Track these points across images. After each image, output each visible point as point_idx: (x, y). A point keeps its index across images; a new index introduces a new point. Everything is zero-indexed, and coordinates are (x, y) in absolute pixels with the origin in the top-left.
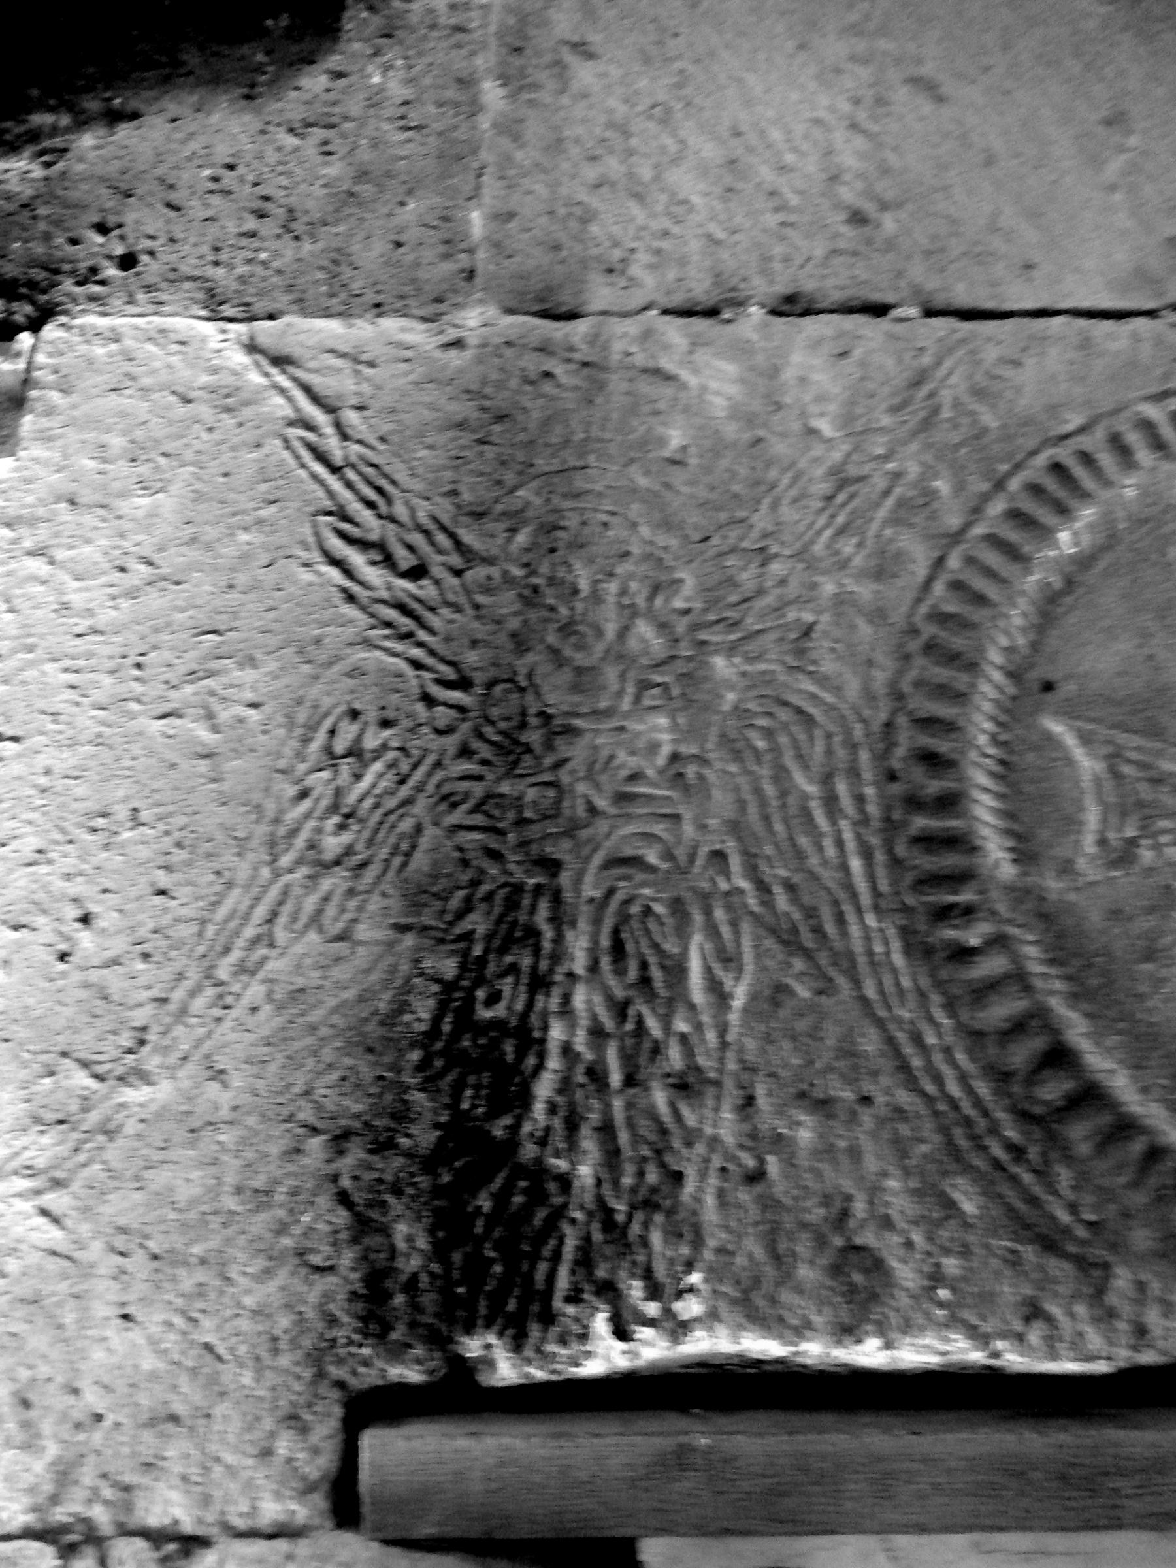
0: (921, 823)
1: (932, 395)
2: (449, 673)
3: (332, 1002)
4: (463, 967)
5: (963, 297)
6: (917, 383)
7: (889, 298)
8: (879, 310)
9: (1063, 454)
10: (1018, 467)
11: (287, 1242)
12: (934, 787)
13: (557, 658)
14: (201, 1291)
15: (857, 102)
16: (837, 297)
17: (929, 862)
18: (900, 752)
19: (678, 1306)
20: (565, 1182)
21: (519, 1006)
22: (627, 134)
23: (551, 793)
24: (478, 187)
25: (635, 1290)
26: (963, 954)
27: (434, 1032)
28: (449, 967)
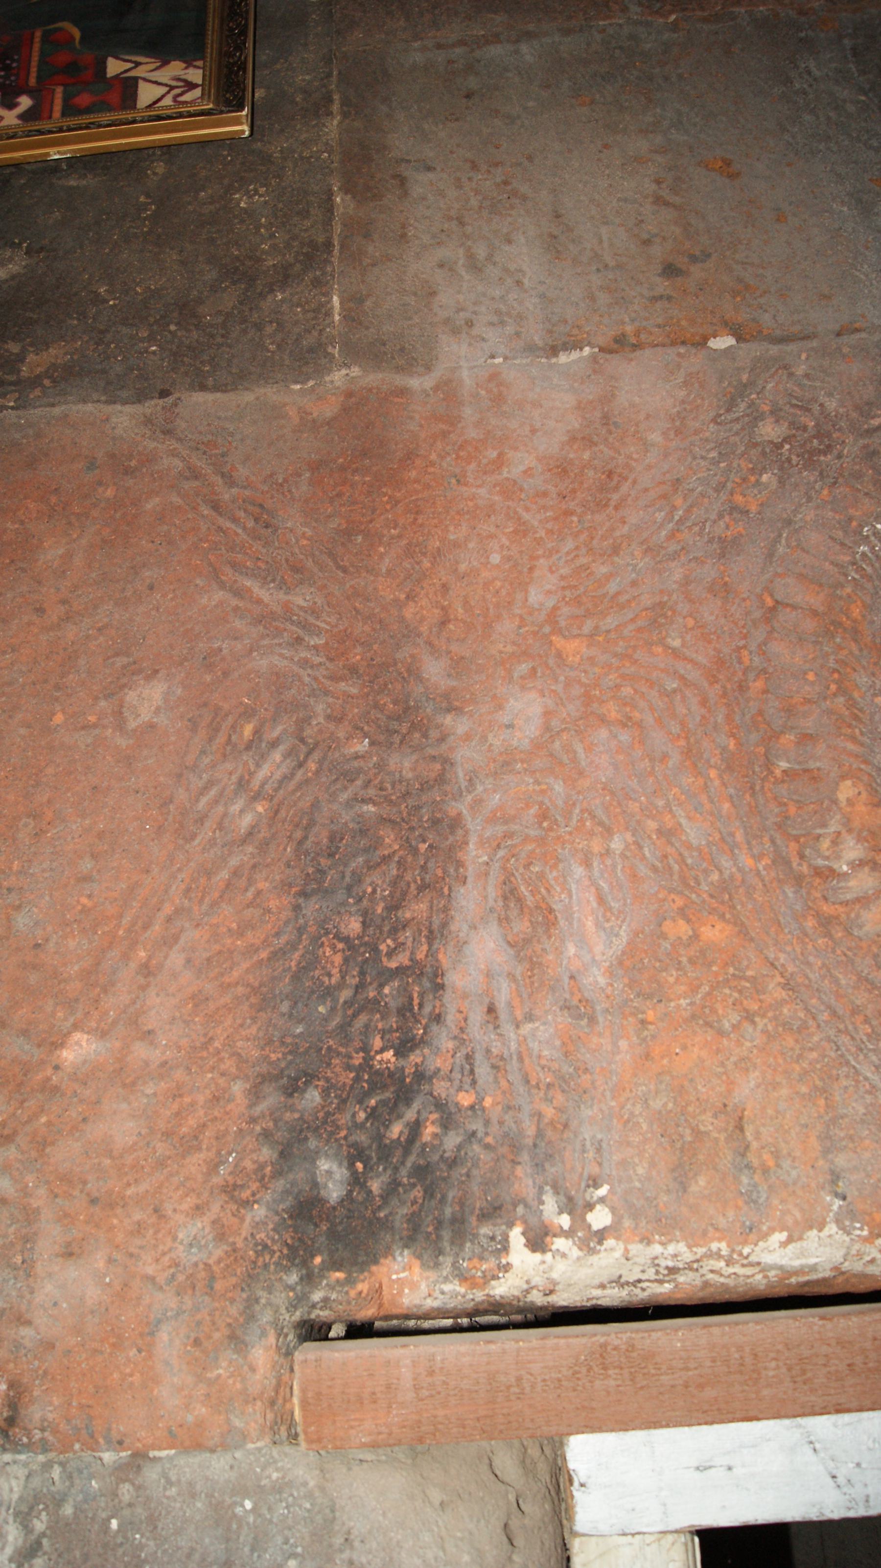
3: (245, 965)
11: (216, 1180)
14: (139, 1229)
15: (658, 182)
19: (590, 1217)
22: (462, 223)
23: (438, 766)
25: (550, 1205)
28: (353, 926)
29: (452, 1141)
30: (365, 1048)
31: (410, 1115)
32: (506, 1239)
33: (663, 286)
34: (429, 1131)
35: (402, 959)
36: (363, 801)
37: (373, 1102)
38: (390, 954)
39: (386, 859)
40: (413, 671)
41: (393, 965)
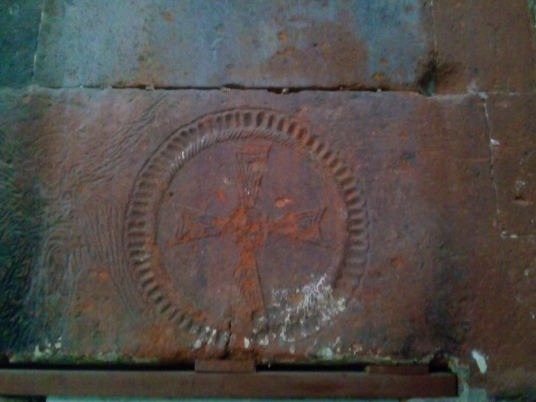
0: (135, 230)
1: (154, 112)
2: (15, 189)
4: (12, 265)
5: (166, 83)
6: (149, 109)
7: (146, 83)
8: (142, 87)
9: (186, 129)
10: (173, 133)
12: (138, 221)
13: (44, 184)
16: (132, 83)
17: (133, 240)
18: (129, 212)
20: (33, 316)
21: (26, 273)
24: (36, 47)
25: (46, 341)
26: (138, 263)
27: (4, 280)
28: (9, 264)
29: (26, 323)
30: (8, 298)
31: (17, 316)
32: (34, 349)
33: (137, 65)
34: (21, 320)
35: (21, 275)
36: (17, 229)
37: (8, 312)
38: (19, 273)
39: (21, 247)
40: (37, 191)
41: (18, 276)
